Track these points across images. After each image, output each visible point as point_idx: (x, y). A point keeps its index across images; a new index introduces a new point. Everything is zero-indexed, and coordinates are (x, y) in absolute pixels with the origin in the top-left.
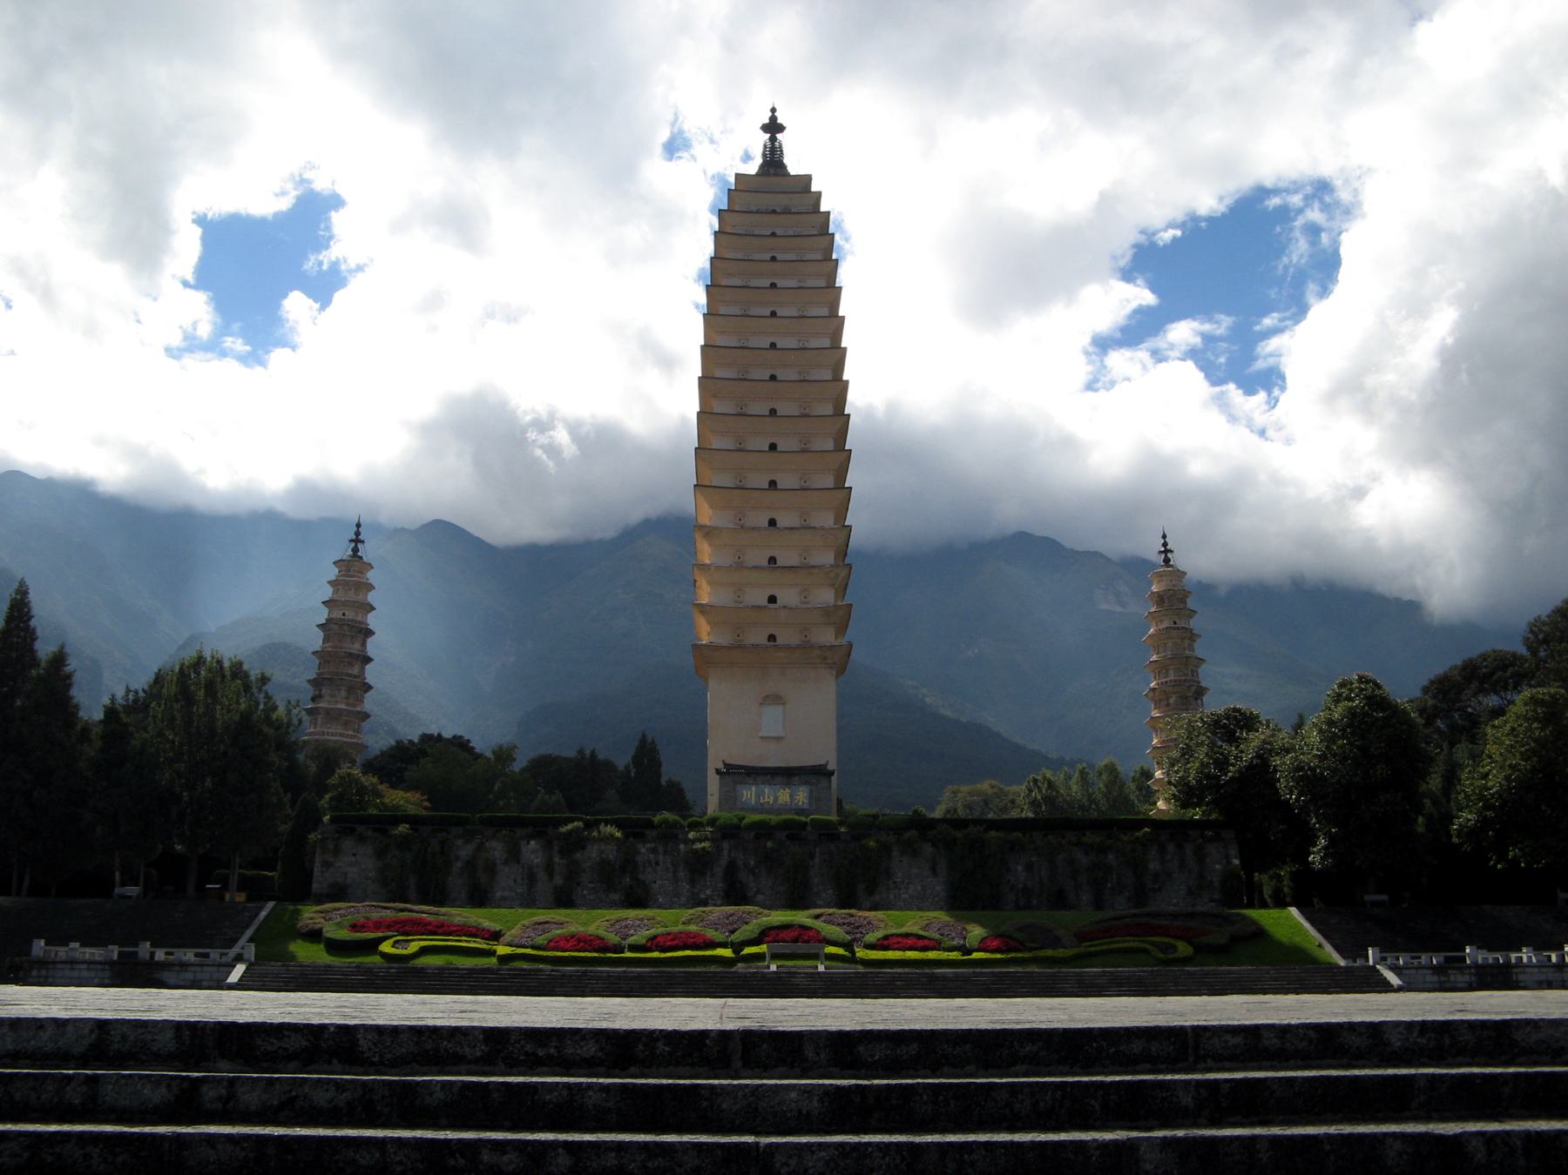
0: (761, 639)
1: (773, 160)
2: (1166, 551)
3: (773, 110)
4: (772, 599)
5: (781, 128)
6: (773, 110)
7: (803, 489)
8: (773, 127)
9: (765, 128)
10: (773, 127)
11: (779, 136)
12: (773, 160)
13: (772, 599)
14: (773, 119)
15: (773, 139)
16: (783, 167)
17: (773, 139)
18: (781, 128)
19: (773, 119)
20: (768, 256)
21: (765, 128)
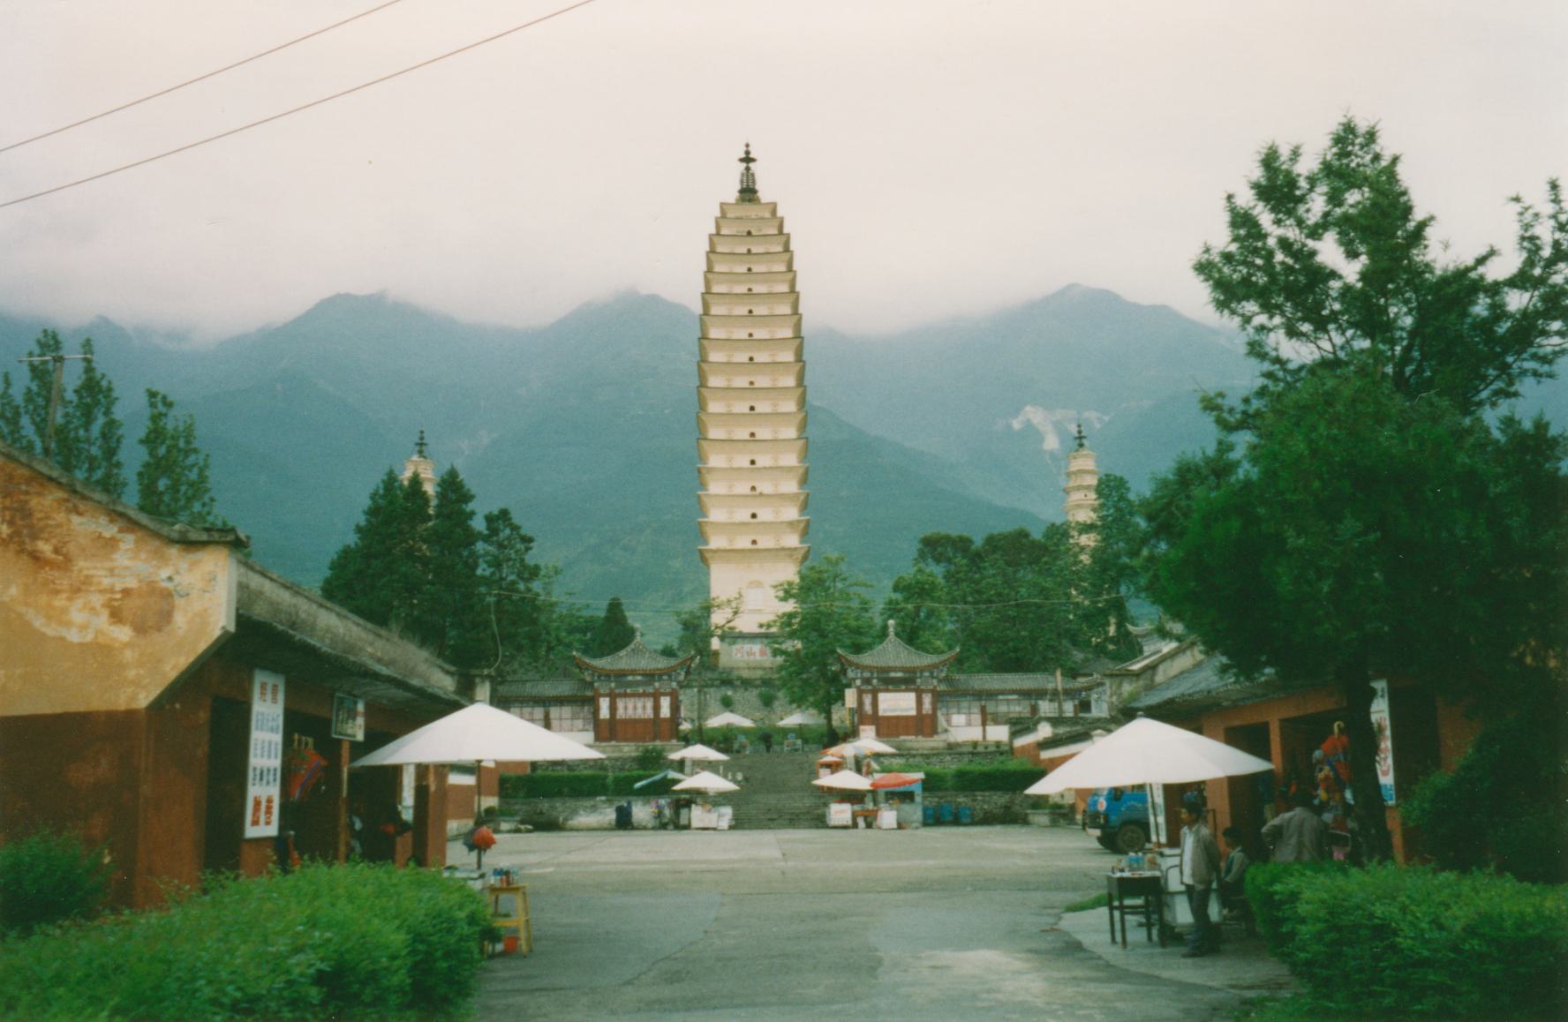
0: (749, 546)
2: (1080, 438)
4: (754, 516)
5: (753, 160)
7: (775, 440)
8: (748, 159)
9: (742, 160)
10: (748, 159)
13: (754, 516)
14: (747, 153)
15: (748, 169)
17: (748, 169)
18: (753, 160)
19: (747, 153)
20: (744, 269)
21: (742, 160)
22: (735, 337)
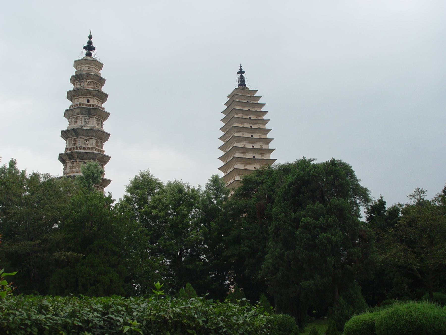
1: (242, 83)
3: (241, 67)
5: (244, 72)
6: (241, 67)
8: (241, 72)
9: (238, 73)
10: (241, 72)
11: (243, 75)
12: (242, 83)
14: (241, 69)
15: (241, 76)
16: (245, 85)
17: (241, 76)
18: (244, 72)
19: (241, 69)
21: (238, 73)
22: (247, 147)
